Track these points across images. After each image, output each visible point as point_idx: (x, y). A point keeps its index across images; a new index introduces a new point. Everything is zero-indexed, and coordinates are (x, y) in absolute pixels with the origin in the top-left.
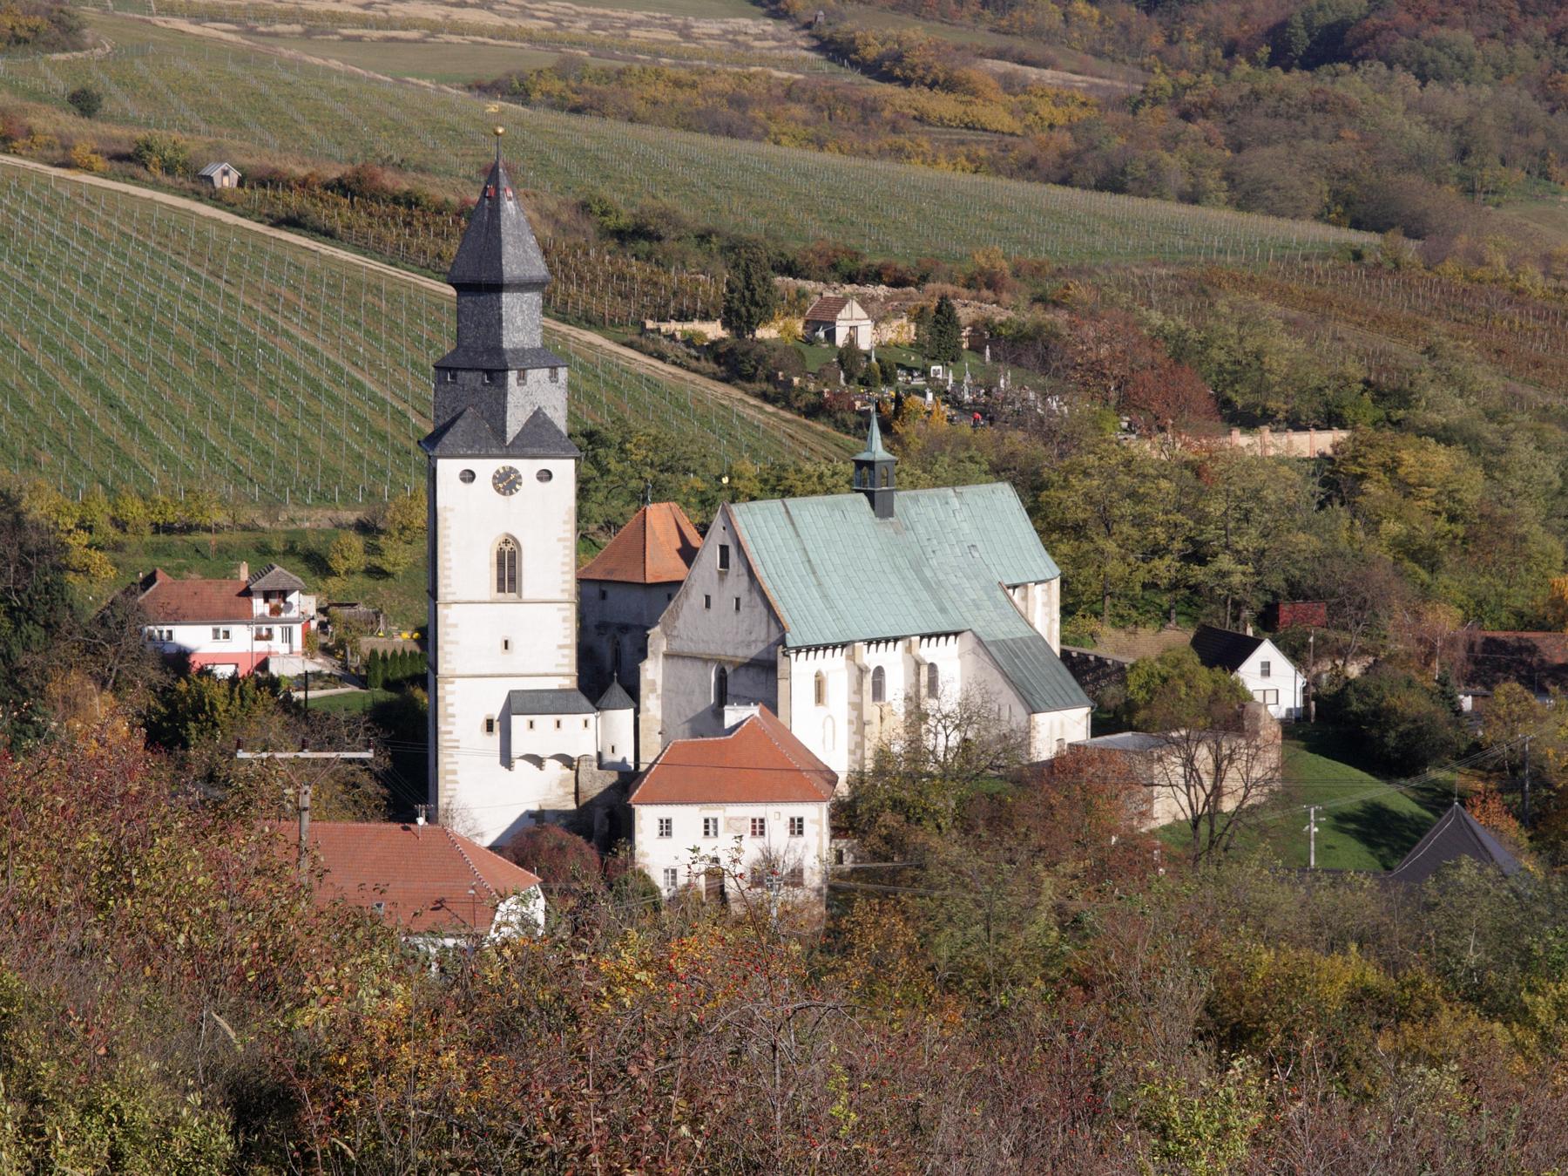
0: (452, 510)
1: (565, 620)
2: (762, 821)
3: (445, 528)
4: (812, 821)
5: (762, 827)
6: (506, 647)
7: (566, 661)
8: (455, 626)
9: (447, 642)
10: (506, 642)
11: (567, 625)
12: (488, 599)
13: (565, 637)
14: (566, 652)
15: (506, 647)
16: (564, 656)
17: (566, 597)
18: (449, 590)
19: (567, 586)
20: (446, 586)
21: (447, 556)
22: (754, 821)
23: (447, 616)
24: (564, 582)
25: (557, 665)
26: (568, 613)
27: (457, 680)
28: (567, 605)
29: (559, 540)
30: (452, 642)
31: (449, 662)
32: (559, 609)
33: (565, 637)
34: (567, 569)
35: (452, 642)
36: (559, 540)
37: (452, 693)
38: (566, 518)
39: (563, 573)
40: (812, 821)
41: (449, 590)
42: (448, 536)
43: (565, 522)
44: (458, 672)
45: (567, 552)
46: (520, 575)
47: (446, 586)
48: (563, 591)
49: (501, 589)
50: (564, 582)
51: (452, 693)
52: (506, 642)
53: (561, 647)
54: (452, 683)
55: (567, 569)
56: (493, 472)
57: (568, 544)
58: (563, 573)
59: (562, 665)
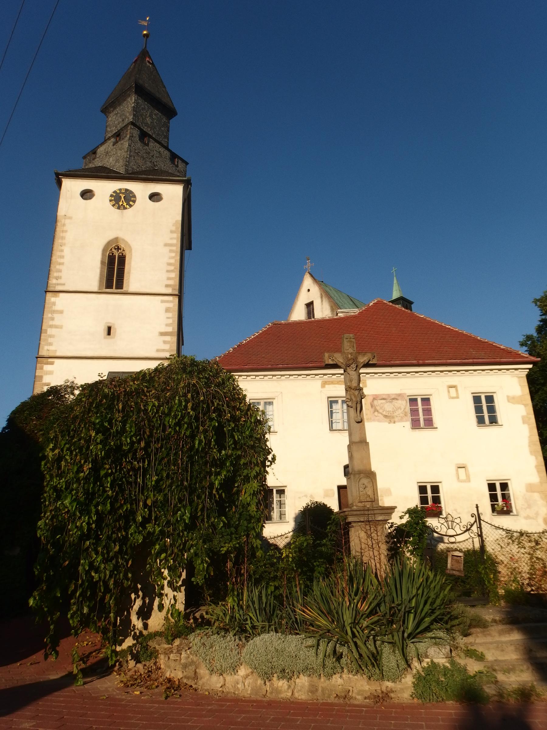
0: (70, 218)
1: (167, 310)
2: (426, 401)
3: (63, 231)
4: (511, 399)
5: (428, 412)
6: (109, 333)
7: (167, 347)
8: (61, 312)
9: (51, 326)
10: (109, 329)
11: (170, 315)
12: (96, 289)
13: (167, 325)
14: (168, 338)
15: (109, 333)
16: (165, 342)
17: (169, 291)
18: (60, 281)
19: (171, 282)
20: (57, 278)
21: (62, 254)
22: (413, 401)
23: (54, 304)
24: (169, 279)
25: (158, 351)
26: (171, 305)
27: (56, 361)
28: (171, 298)
29: (166, 245)
30: (56, 327)
31: (50, 344)
32: (163, 302)
33: (167, 325)
34: (172, 268)
35: (56, 327)
36: (166, 245)
37: (51, 373)
38: (174, 228)
39: (168, 271)
40: (511, 399)
41: (60, 281)
42: (63, 238)
43: (172, 232)
44: (58, 354)
45: (173, 255)
46: (129, 273)
47: (57, 278)
48: (167, 286)
49: (109, 285)
50: (169, 279)
51: (51, 373)
52: (109, 329)
53: (162, 334)
54: (52, 363)
55: (172, 268)
56: (111, 192)
57: (174, 248)
58: (168, 271)
59: (163, 350)
